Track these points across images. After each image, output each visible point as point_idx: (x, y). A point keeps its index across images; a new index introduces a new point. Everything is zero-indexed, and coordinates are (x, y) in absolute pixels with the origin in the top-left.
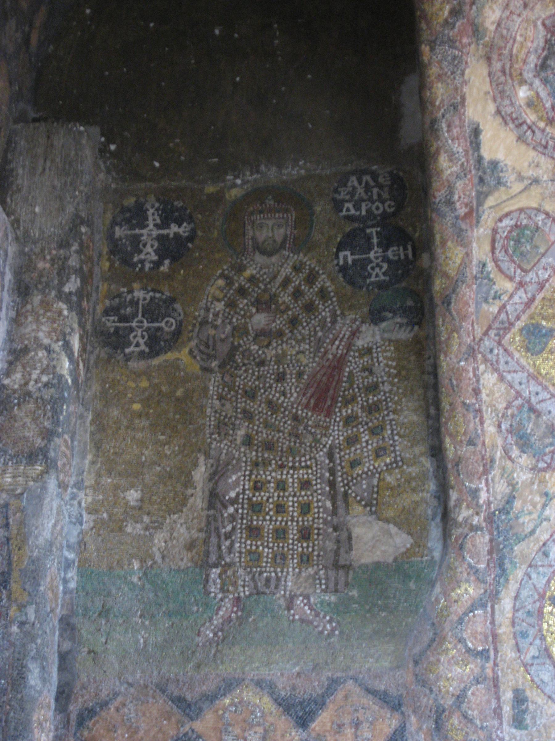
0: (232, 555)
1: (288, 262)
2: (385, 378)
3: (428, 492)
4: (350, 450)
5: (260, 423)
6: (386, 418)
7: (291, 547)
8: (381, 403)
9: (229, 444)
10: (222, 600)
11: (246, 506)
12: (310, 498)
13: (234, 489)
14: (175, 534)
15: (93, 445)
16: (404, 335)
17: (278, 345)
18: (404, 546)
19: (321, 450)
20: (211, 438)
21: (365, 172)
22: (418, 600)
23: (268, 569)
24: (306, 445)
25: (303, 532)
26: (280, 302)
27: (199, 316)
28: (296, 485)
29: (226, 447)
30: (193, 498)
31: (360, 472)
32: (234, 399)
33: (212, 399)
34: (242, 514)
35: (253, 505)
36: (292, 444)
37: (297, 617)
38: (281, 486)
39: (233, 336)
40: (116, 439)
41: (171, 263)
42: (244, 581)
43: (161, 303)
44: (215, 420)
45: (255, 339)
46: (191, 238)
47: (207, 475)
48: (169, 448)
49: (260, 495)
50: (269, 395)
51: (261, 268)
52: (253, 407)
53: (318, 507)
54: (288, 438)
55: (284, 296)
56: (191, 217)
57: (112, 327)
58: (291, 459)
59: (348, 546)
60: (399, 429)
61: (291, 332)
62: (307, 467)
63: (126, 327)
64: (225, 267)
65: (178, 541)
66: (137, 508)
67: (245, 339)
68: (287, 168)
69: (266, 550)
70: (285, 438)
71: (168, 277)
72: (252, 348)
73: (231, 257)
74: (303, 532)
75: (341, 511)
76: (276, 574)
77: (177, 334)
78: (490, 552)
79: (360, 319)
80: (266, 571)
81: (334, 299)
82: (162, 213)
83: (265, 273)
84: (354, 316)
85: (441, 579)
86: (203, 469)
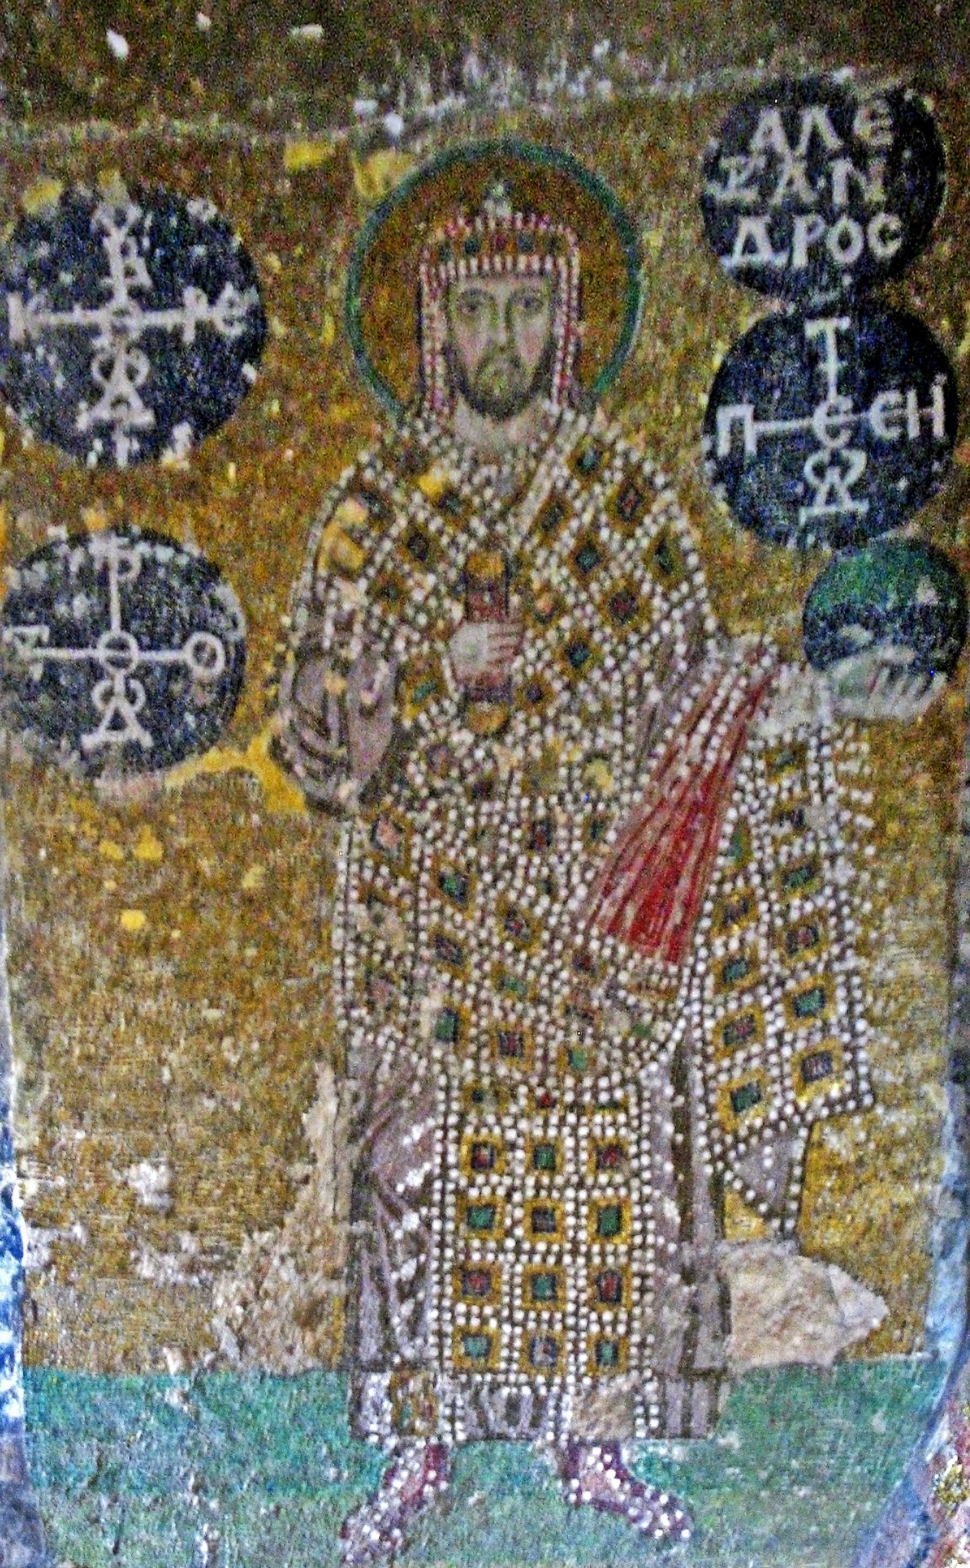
0: (419, 1341)
1: (559, 440)
2: (839, 844)
3: (936, 1180)
4: (732, 1059)
5: (484, 977)
6: (837, 967)
7: (571, 1321)
8: (825, 922)
9: (399, 1036)
10: (397, 1452)
11: (450, 1212)
12: (623, 1192)
13: (417, 1165)
14: (268, 1284)
15: (22, 1033)
17: (530, 732)
18: (865, 1323)
19: (653, 1059)
20: (347, 1016)
22: (891, 1458)
23: (512, 1378)
24: (611, 1043)
25: (603, 1284)
26: (536, 585)
27: (294, 628)
28: (584, 1156)
29: (392, 1046)
30: (310, 1187)
31: (758, 1123)
32: (407, 900)
33: (346, 902)
34: (442, 1233)
35: (469, 1210)
36: (574, 1038)
37: (587, 1496)
39: (398, 699)
40: (84, 1018)
41: (195, 440)
42: (453, 1406)
43: (175, 583)
44: (357, 965)
45: (462, 710)
47: (343, 1123)
48: (235, 1046)
49: (487, 1183)
50: (506, 890)
51: (476, 463)
52: (462, 927)
53: (643, 1218)
54: (562, 1022)
55: (546, 563)
56: (246, 263)
57: (35, 660)
58: (569, 1082)
59: (718, 1323)
60: (870, 999)
61: (569, 687)
62: (615, 1106)
63: (79, 663)
64: (364, 457)
65: (276, 1303)
66: (162, 1213)
67: (434, 709)
68: (554, 69)
69: (507, 1328)
70: (553, 1022)
72: (455, 738)
73: (381, 418)
74: (603, 1284)
75: (704, 1229)
76: (535, 1390)
79: (774, 650)
80: (506, 1383)
81: (700, 578)
82: (153, 246)
83: (488, 482)
84: (756, 639)
85: (952, 1409)
86: (332, 1107)
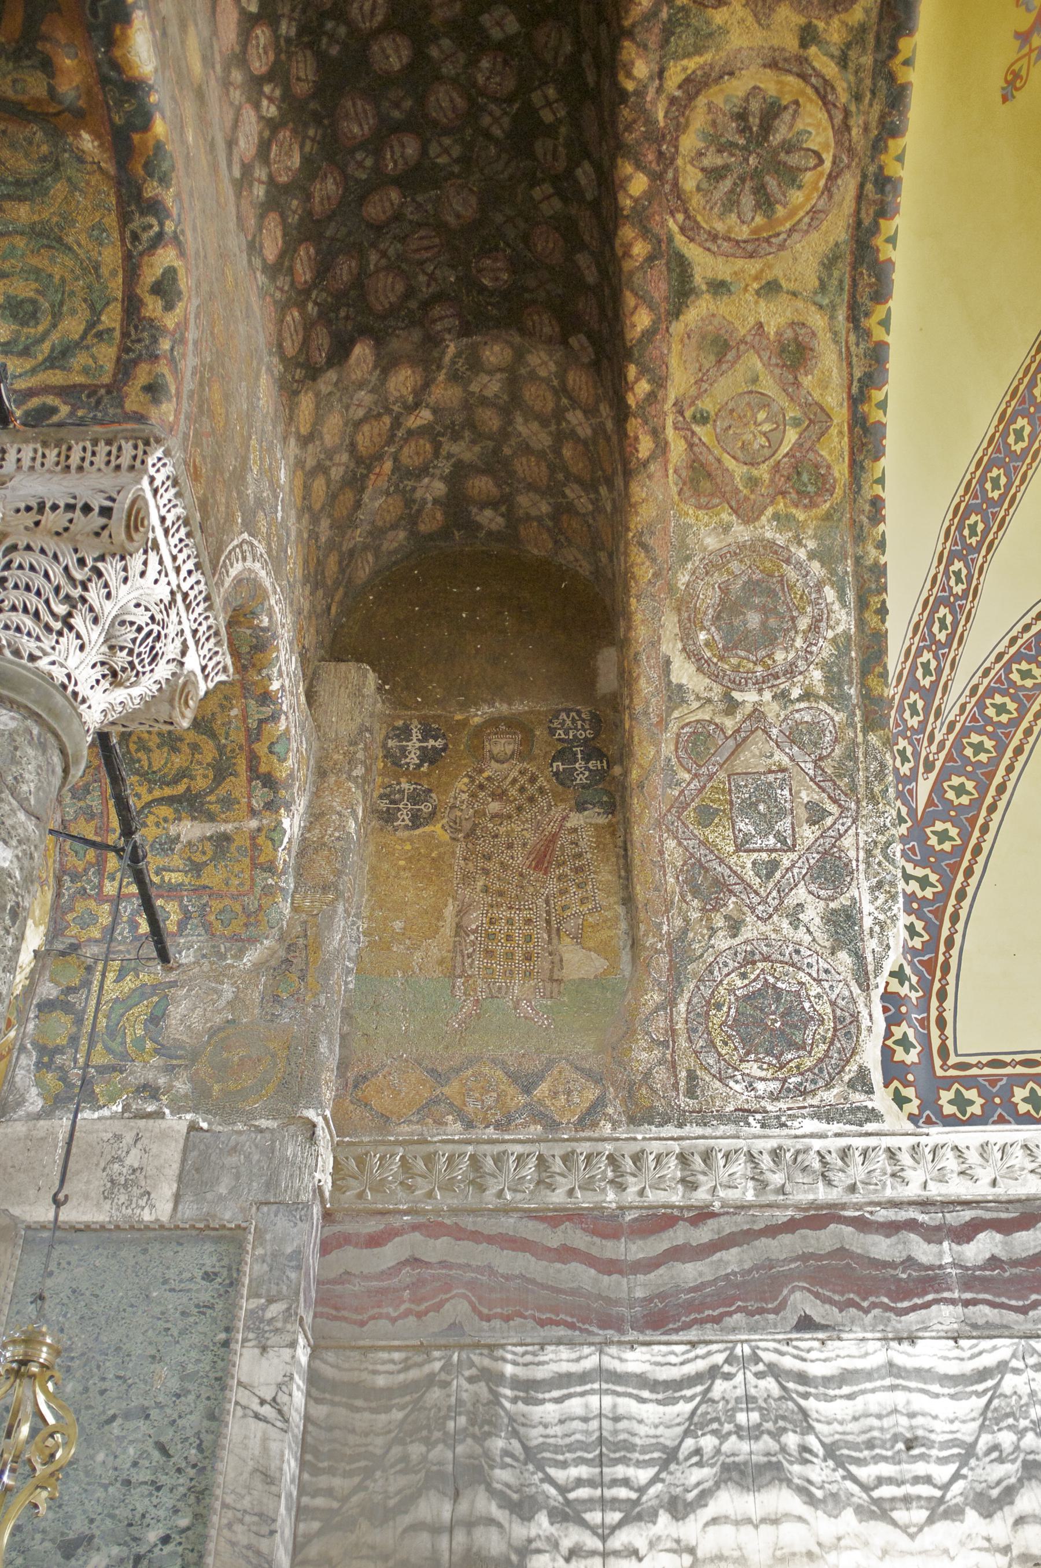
16: (602, 820)
21: (572, 710)
38: (510, 922)
46: (444, 749)
71: (428, 775)
75: (555, 941)
77: (433, 814)
78: (669, 970)
